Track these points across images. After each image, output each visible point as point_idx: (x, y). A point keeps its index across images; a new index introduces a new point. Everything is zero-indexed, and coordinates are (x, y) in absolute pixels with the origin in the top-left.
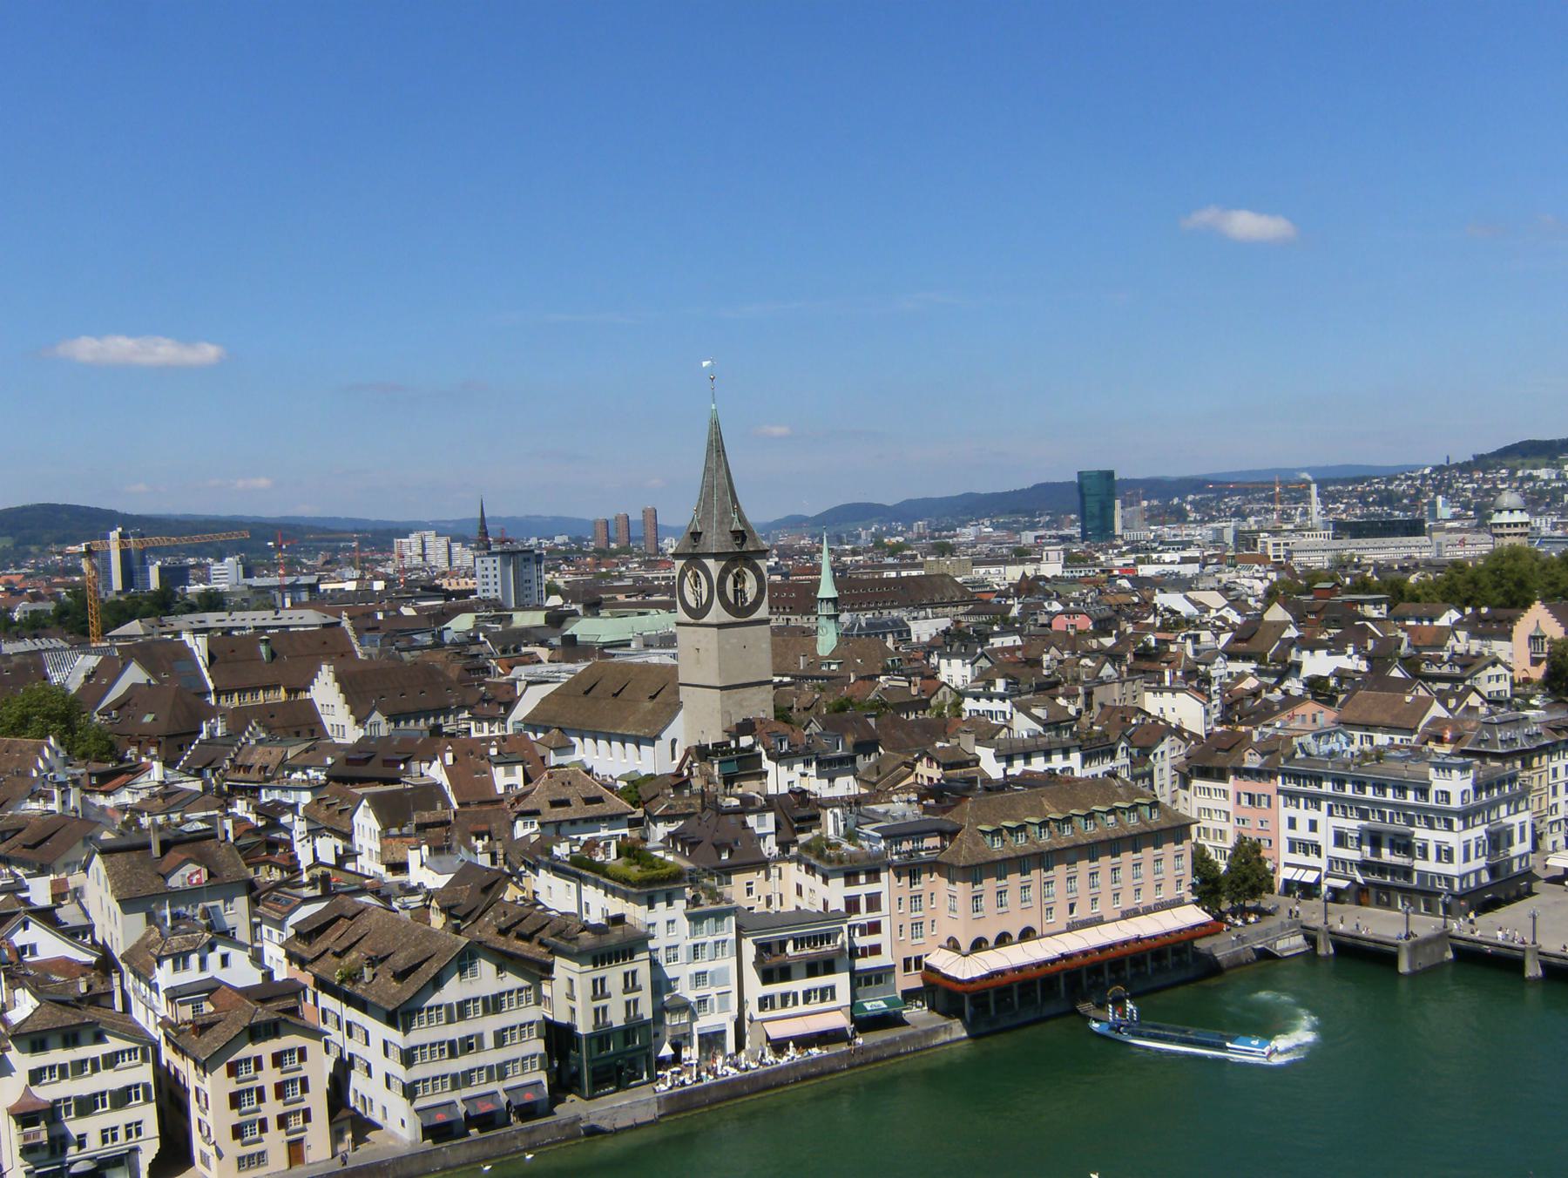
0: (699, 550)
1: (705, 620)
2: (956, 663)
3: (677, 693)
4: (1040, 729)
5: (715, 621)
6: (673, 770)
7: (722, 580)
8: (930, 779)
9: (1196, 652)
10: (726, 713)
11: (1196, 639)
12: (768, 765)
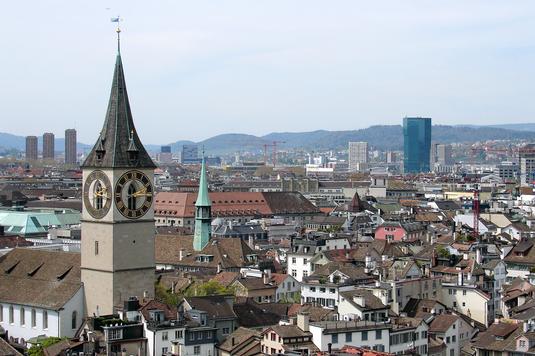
0: (104, 164)
1: (105, 219)
2: (300, 260)
3: (79, 275)
4: (360, 314)
5: (112, 220)
6: (72, 336)
7: (118, 190)
8: (273, 350)
9: (483, 261)
10: (117, 294)
11: (484, 251)
12: (149, 334)
